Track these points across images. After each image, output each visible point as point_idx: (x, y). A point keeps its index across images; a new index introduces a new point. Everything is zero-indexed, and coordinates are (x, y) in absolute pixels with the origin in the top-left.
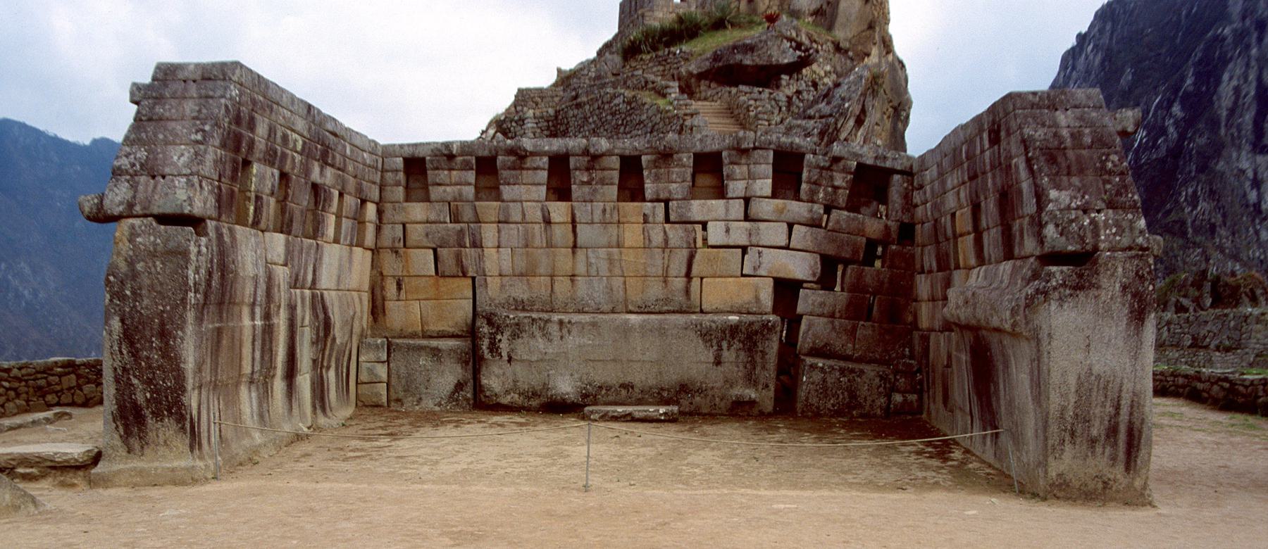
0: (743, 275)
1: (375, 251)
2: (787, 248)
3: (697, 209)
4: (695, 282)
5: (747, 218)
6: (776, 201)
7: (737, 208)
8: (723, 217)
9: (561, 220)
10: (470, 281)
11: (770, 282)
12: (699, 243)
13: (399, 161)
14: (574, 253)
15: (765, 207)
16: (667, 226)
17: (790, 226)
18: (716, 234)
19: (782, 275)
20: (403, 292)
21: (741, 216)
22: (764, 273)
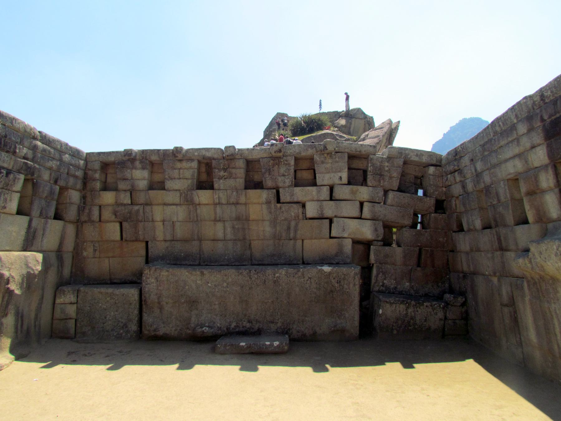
0: (331, 237)
1: (79, 223)
2: (360, 218)
3: (300, 193)
4: (299, 243)
5: (331, 199)
6: (351, 186)
7: (325, 192)
8: (316, 198)
9: (207, 202)
10: (144, 244)
11: (350, 240)
12: (301, 216)
13: (97, 166)
14: (215, 224)
15: (342, 192)
16: (279, 205)
17: (362, 204)
18: (311, 210)
19: (359, 237)
20: (97, 253)
21: (328, 198)
22: (346, 235)
